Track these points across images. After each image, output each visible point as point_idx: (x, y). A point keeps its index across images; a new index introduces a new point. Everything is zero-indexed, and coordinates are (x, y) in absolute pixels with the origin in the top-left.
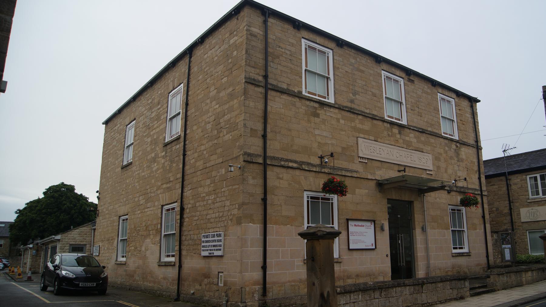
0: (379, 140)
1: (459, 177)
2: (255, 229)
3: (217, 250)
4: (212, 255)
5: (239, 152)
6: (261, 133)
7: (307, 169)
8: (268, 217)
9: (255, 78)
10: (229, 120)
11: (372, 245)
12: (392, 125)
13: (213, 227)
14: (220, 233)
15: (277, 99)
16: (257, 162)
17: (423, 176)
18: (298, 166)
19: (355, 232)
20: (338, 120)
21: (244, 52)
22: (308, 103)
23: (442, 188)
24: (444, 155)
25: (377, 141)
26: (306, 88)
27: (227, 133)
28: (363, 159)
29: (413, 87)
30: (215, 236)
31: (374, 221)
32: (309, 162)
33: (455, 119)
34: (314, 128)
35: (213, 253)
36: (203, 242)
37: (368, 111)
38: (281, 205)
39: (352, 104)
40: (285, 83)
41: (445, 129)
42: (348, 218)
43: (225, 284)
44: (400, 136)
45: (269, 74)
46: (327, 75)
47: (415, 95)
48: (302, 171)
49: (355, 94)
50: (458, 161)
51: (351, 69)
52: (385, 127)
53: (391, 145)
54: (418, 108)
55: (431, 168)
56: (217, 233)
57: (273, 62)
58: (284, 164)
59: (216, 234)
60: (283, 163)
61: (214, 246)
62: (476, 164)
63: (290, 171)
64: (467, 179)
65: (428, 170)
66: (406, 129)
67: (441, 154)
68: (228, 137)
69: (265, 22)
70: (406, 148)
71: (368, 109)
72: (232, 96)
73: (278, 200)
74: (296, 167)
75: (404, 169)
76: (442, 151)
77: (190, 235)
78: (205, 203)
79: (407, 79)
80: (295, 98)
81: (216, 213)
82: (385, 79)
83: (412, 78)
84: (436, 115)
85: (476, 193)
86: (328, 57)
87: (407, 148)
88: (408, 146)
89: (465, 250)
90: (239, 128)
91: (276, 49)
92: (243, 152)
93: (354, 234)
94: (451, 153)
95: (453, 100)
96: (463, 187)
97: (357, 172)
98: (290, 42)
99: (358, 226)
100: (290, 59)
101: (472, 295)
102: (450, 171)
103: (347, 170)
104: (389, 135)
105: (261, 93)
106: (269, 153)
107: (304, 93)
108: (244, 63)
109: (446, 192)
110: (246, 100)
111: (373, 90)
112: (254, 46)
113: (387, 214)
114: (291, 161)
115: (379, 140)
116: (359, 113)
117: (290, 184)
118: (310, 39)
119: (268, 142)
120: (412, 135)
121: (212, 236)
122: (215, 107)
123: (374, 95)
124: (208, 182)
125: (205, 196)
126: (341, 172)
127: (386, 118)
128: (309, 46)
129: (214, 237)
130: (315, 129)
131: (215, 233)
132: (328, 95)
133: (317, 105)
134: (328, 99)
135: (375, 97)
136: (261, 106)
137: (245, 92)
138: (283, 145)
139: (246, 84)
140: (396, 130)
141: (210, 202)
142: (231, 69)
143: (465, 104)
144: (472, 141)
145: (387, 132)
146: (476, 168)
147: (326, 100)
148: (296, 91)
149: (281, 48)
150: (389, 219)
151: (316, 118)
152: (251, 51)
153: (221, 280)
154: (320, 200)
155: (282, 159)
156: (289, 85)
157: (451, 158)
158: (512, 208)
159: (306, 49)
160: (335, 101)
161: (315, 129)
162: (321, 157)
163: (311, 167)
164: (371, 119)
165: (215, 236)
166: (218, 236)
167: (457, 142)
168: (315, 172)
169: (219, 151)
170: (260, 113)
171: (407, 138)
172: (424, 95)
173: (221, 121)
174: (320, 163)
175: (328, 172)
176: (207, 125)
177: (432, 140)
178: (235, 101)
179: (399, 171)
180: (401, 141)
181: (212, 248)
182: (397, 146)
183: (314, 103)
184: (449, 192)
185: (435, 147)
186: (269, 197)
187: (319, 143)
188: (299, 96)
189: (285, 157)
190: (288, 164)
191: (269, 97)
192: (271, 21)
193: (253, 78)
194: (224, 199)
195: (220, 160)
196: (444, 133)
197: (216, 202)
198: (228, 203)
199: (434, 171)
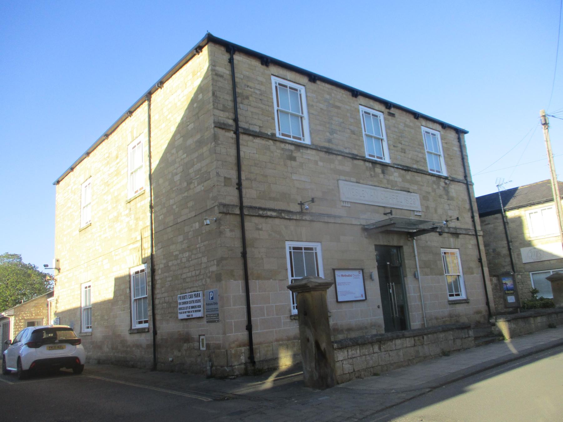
0: (361, 181)
1: (451, 217)
2: (237, 286)
3: (196, 311)
4: (191, 317)
5: (213, 204)
6: (235, 180)
7: (286, 217)
8: (249, 272)
9: (225, 122)
10: (200, 170)
11: (362, 295)
12: (374, 164)
13: (190, 287)
14: (198, 292)
15: (250, 143)
16: (234, 213)
17: (411, 218)
18: (277, 215)
19: (342, 283)
20: (316, 163)
21: (210, 94)
22: (283, 145)
23: (434, 229)
24: (433, 194)
25: (359, 183)
26: (279, 130)
27: (198, 184)
28: (345, 203)
29: (394, 121)
30: (193, 296)
31: (362, 270)
32: (289, 209)
33: (442, 154)
34: (291, 173)
35: (192, 315)
36: (180, 303)
37: (347, 151)
38: (262, 259)
39: (330, 144)
40: (256, 125)
41: (431, 165)
42: (334, 267)
43: (208, 346)
44: (384, 176)
45: (239, 116)
46: (301, 114)
47: (396, 130)
48: (283, 220)
49: (332, 132)
50: (448, 199)
51: (327, 106)
52: (367, 167)
53: (375, 186)
54: (401, 144)
55: (419, 209)
56: (195, 293)
57: (242, 103)
58: (263, 213)
59: (194, 294)
60: (261, 212)
61: (192, 307)
62: (468, 201)
63: (269, 220)
64: (460, 219)
65: (416, 211)
66: (389, 167)
67: (429, 193)
68: (200, 188)
69: (231, 61)
70: (391, 189)
71: (348, 149)
72: (200, 143)
73: (259, 253)
74: (275, 216)
75: (390, 212)
76: (430, 190)
77: (165, 298)
78: (179, 261)
79: (387, 113)
80: (269, 142)
81: (192, 271)
82: (363, 114)
83: (393, 110)
84: (421, 150)
85: (470, 233)
86: (300, 95)
87: (392, 188)
88: (392, 186)
89: (463, 296)
90: (211, 178)
91: (245, 89)
92: (218, 203)
94: (440, 191)
95: (438, 132)
96: (455, 228)
97: (340, 217)
98: (258, 81)
99: (345, 276)
100: (260, 99)
101: (478, 346)
102: (440, 211)
103: (329, 216)
104: (371, 175)
105: (232, 138)
106: (246, 203)
107: (278, 135)
108: (212, 107)
109: (437, 234)
110: (217, 146)
111: (352, 128)
112: (221, 87)
113: (376, 261)
114: (270, 210)
116: (339, 153)
118: (280, 76)
119: (244, 191)
120: (396, 174)
121: (190, 297)
122: (183, 157)
123: (353, 132)
124: (181, 238)
125: (178, 253)
127: (367, 157)
128: (280, 84)
129: (192, 298)
130: (292, 174)
131: (193, 293)
132: (303, 136)
133: (292, 148)
134: (304, 140)
135: (354, 134)
136: (233, 152)
137: (215, 138)
138: (260, 193)
139: (216, 129)
140: (378, 170)
141: (184, 260)
142: (197, 113)
143: (452, 135)
144: (461, 177)
145: (370, 173)
146: (467, 206)
147: (302, 142)
148: (269, 133)
149: (251, 88)
150: (378, 267)
151: (292, 162)
152: (218, 92)
153: (203, 344)
154: (303, 251)
155: (260, 209)
156: (262, 127)
157: (440, 196)
158: (511, 249)
159: (276, 87)
160: (312, 142)
161: (292, 174)
162: (301, 204)
164: (351, 160)
165: (193, 296)
166: (196, 297)
167: (446, 178)
169: (191, 204)
170: (233, 159)
171: (391, 178)
172: (406, 129)
173: (191, 171)
174: (300, 210)
175: (310, 220)
176: (175, 177)
177: (419, 178)
178: (205, 149)
179: (385, 214)
180: (385, 181)
181: (191, 310)
182: (381, 187)
183: (290, 145)
184: (440, 234)
185: (422, 186)
186: (248, 250)
187: (298, 188)
188: (273, 138)
189: (263, 206)
190: (267, 213)
191: (241, 142)
192: (238, 58)
193: (222, 122)
194: (200, 255)
195: (193, 214)
196: (431, 170)
197: (192, 260)
198: (205, 260)
199: (423, 212)
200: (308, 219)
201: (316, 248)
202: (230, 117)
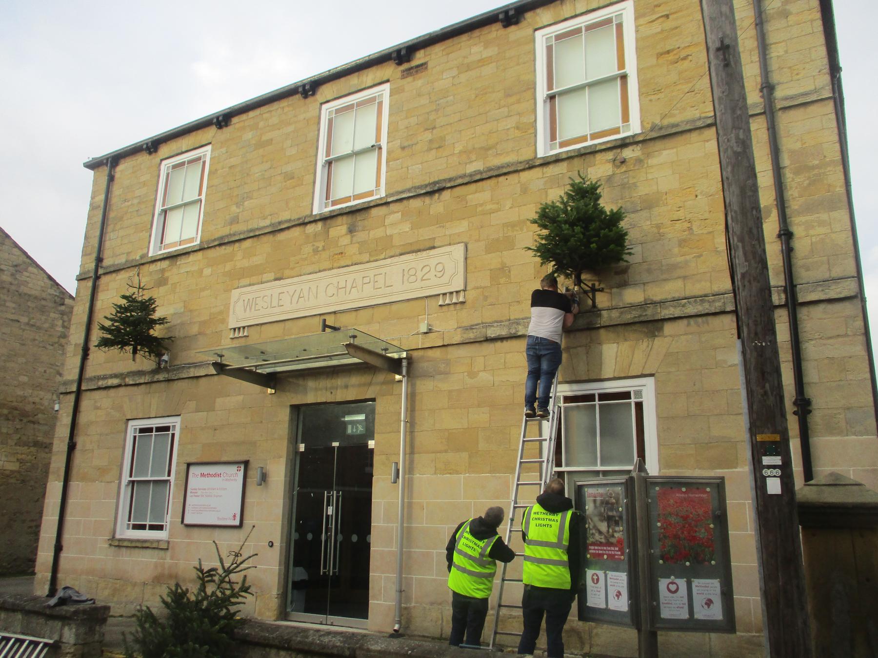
7: (131, 382)
11: (235, 516)
19: (199, 489)
63: (112, 392)
93: (196, 493)
115: (287, 272)
148: (138, 258)
163: (137, 379)
164: (272, 236)
180: (353, 250)
182: (339, 268)
200: (161, 379)
202: (88, 261)
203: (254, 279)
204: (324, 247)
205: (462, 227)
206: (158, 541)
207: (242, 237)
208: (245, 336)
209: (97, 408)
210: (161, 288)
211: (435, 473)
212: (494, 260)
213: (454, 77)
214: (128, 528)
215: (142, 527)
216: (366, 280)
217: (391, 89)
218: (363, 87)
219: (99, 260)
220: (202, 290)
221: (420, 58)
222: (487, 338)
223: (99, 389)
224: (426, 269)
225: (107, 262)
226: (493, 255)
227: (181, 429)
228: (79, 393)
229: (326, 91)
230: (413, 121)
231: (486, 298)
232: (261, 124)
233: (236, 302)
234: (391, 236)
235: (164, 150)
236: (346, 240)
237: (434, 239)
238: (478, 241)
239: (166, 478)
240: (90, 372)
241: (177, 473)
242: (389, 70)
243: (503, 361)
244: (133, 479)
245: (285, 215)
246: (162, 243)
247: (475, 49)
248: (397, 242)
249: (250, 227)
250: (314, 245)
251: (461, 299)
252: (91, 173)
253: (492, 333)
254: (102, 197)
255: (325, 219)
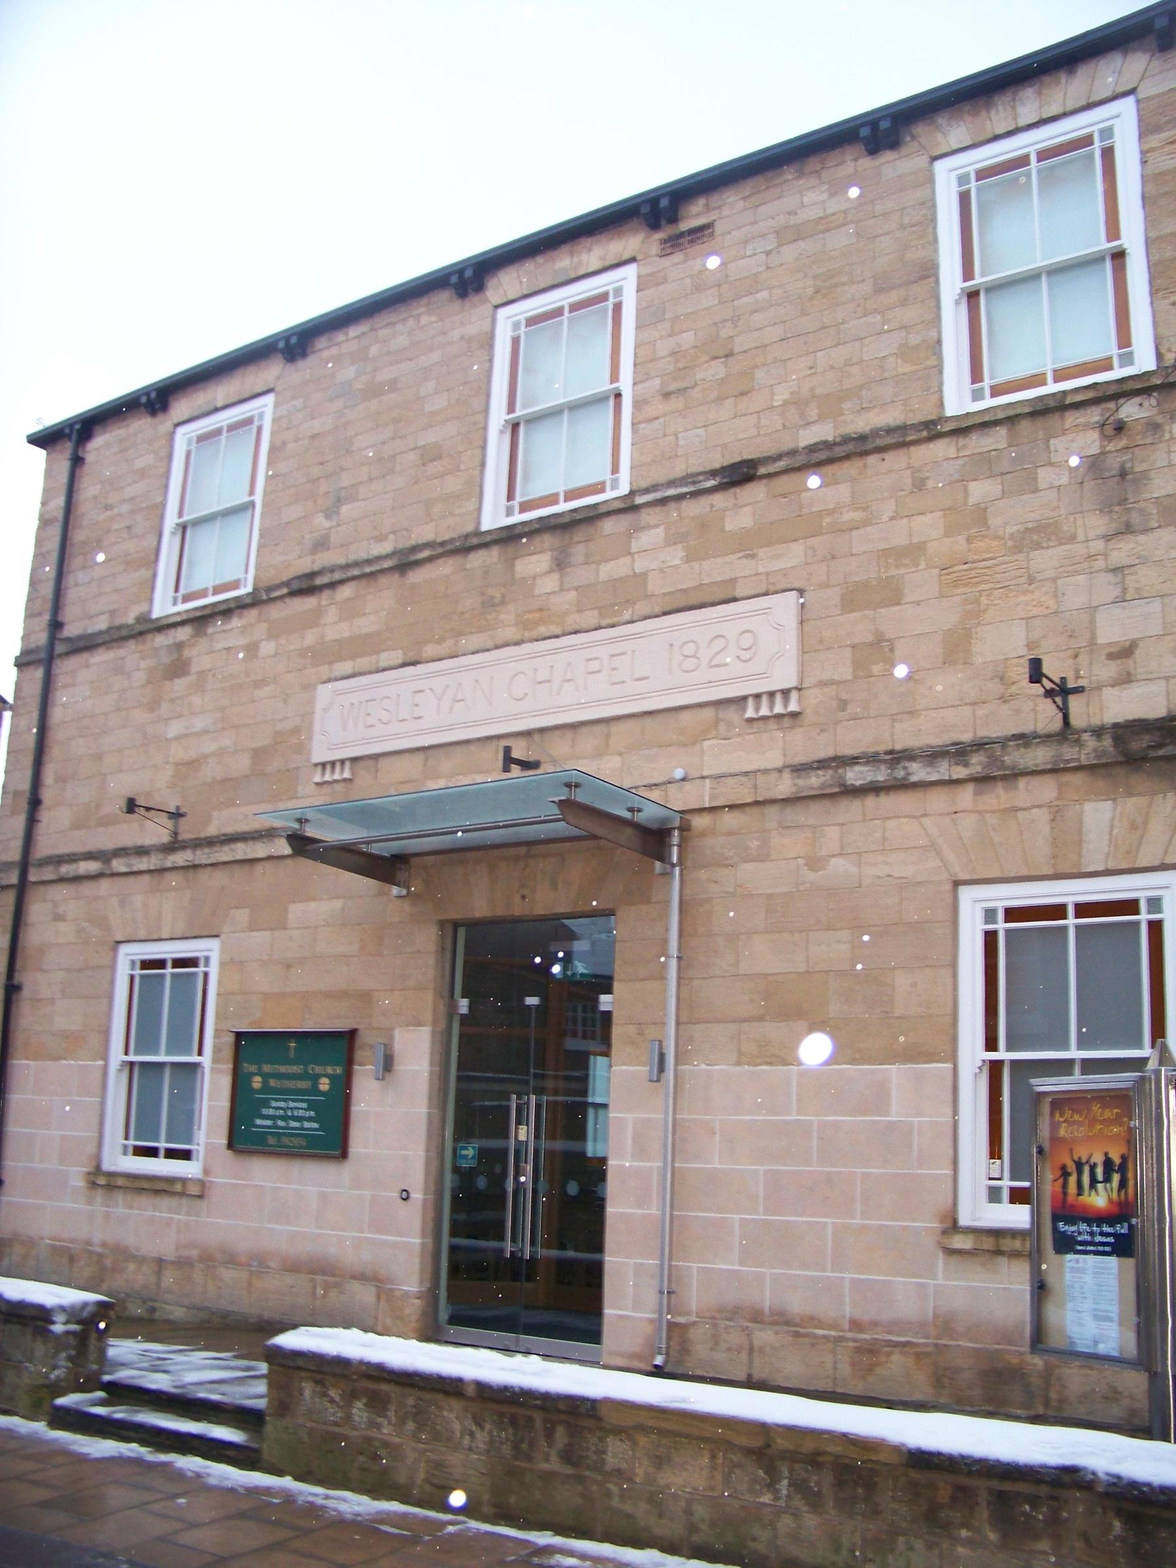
7: (123, 869)
63: (87, 889)
115: (429, 650)
117: (80, 931)
126: (232, 850)
168: (150, 871)
200: (181, 863)
201: (207, 959)
202: (37, 628)
203: (363, 663)
204: (503, 596)
205: (794, 555)
206: (184, 1181)
207: (337, 576)
208: (345, 780)
209: (58, 918)
210: (177, 681)
211: (739, 1063)
212: (859, 627)
213: (768, 253)
214: (125, 1153)
215: (152, 1152)
216: (594, 666)
217: (639, 277)
218: (582, 272)
219: (56, 625)
220: (259, 684)
221: (698, 215)
222: (843, 785)
223: (62, 880)
224: (719, 644)
225: (72, 630)
226: (857, 614)
227: (223, 965)
228: (22, 889)
229: (506, 282)
230: (687, 339)
231: (843, 704)
232: (374, 350)
233: (325, 710)
234: (644, 575)
235: (181, 407)
236: (550, 583)
237: (733, 581)
238: (825, 586)
239: (194, 1058)
240: (45, 846)
241: (217, 1050)
242: (632, 242)
243: (878, 835)
244: (132, 1058)
245: (426, 533)
246: (177, 590)
247: (810, 197)
248: (656, 585)
249: (352, 558)
250: (483, 594)
251: (793, 707)
252: (40, 454)
253: (855, 776)
254: (60, 501)
255: (509, 537)
